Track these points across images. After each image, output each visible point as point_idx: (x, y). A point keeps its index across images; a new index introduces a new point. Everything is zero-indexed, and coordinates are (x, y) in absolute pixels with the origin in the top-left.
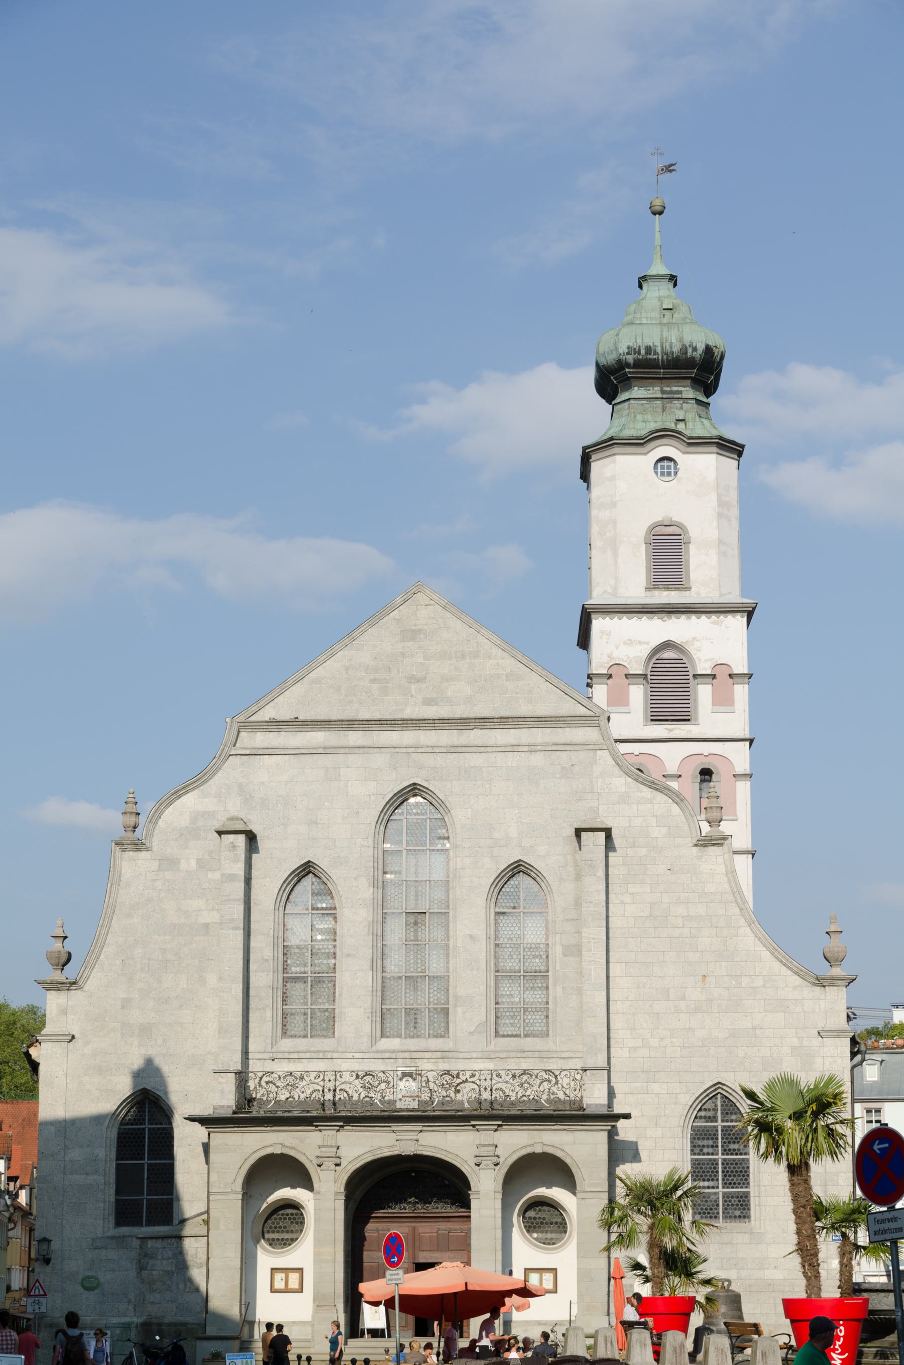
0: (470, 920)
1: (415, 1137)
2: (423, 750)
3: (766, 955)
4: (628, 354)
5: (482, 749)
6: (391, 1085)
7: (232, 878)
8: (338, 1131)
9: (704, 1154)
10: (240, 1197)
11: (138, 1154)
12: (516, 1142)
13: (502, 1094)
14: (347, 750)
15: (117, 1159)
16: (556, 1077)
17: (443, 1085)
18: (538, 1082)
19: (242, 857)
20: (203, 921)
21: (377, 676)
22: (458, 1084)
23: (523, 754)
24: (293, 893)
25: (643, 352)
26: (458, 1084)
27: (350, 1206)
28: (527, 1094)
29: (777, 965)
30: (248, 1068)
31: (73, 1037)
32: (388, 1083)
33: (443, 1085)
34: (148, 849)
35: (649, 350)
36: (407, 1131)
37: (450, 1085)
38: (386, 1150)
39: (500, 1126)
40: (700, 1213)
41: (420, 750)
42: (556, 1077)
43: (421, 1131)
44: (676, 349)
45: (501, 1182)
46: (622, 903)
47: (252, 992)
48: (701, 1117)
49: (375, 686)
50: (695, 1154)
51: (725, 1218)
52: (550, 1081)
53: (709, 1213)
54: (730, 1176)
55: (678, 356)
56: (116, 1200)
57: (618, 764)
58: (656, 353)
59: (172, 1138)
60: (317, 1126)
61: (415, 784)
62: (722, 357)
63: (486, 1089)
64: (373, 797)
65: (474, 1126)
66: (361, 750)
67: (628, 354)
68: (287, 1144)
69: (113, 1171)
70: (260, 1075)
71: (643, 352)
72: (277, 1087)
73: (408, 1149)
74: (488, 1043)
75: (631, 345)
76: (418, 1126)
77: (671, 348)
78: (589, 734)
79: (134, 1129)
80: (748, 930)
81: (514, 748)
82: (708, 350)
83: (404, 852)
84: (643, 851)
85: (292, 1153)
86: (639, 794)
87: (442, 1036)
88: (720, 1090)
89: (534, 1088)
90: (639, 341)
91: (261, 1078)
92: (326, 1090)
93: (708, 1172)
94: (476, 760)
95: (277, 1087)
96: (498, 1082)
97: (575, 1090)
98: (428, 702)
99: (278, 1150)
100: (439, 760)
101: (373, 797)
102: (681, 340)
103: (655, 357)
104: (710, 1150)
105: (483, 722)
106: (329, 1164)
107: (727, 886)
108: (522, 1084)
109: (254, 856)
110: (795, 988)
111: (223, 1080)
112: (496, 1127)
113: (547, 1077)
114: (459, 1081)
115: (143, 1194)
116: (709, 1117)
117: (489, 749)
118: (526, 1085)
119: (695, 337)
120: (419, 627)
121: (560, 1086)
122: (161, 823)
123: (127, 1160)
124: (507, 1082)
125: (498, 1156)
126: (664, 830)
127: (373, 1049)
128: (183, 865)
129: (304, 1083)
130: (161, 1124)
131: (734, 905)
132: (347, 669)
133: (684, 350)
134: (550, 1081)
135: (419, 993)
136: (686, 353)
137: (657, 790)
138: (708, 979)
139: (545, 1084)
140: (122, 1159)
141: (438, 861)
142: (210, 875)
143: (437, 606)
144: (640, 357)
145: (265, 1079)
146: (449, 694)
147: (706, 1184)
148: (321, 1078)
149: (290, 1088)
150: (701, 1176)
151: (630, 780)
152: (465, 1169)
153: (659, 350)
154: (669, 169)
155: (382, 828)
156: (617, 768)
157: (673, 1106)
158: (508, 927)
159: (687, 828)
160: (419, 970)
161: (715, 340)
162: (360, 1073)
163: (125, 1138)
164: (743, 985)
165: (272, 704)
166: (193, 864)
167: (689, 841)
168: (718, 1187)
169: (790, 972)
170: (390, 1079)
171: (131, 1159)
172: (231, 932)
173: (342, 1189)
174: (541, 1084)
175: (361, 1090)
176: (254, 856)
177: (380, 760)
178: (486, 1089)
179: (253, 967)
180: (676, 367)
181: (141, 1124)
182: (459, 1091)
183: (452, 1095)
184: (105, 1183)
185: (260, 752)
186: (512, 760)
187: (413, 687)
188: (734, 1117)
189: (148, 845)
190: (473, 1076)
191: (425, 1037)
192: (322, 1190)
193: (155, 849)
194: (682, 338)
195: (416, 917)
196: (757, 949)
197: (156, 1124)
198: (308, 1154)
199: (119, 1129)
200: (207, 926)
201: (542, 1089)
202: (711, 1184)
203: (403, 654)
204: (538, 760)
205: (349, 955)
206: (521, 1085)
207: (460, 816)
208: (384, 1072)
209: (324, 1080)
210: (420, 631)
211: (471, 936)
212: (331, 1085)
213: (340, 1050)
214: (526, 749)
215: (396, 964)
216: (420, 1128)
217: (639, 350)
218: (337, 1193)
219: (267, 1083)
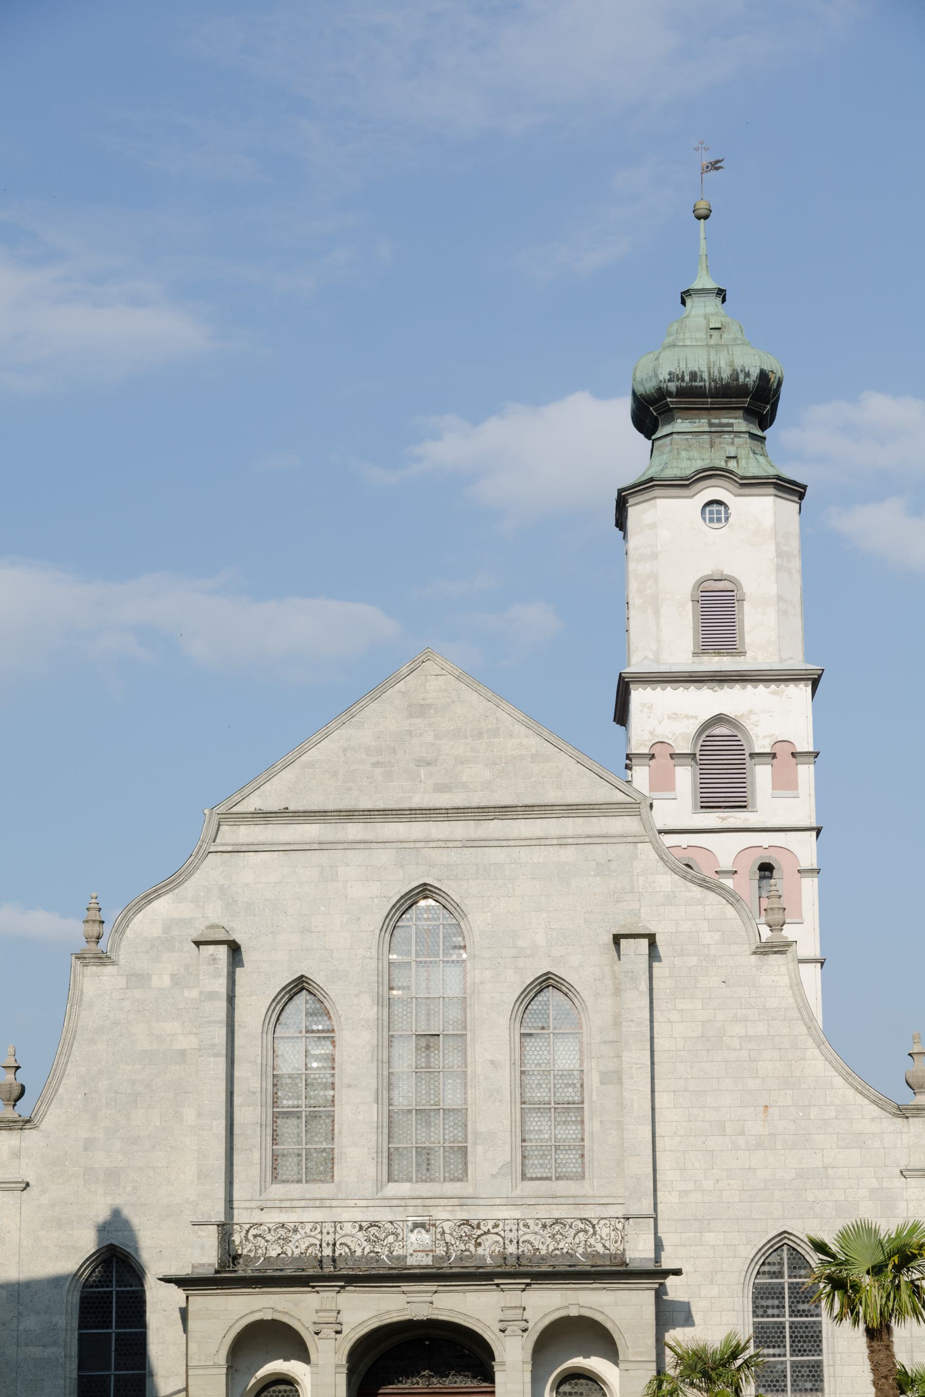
0: (491, 1043)
1: (429, 1299)
2: (434, 844)
3: (839, 1081)
4: (670, 381)
5: (503, 843)
6: (400, 1238)
7: (212, 996)
8: (339, 1292)
9: (768, 1316)
10: (224, 1371)
11: (105, 1322)
12: (547, 1304)
13: (530, 1248)
14: (346, 846)
15: (80, 1328)
16: (594, 1227)
17: (461, 1237)
19: (224, 971)
20: (179, 1047)
21: (380, 758)
22: (479, 1236)
23: (551, 849)
24: (284, 1014)
25: (687, 378)
26: (479, 1236)
27: (353, 1380)
28: (560, 1247)
29: (851, 1092)
30: (232, 1219)
31: (28, 1185)
32: (397, 1235)
33: (461, 1237)
34: (113, 963)
35: (694, 376)
36: (419, 1292)
37: (469, 1236)
38: (394, 1315)
39: (528, 1284)
40: (764, 1386)
41: (431, 844)
42: (594, 1227)
43: (436, 1292)
44: (726, 375)
45: (530, 1351)
46: (669, 1021)
47: (237, 1130)
48: (764, 1273)
49: (378, 770)
51: (794, 1391)
52: (586, 1231)
53: (775, 1386)
54: (799, 1341)
55: (727, 383)
56: (79, 1376)
57: (662, 859)
58: (702, 380)
59: (145, 1302)
60: (313, 1287)
61: (425, 884)
62: (780, 384)
63: (511, 1241)
64: (376, 901)
65: (497, 1285)
66: (362, 845)
67: (670, 381)
68: (279, 1308)
69: (75, 1342)
70: (247, 1227)
71: (687, 378)
72: (267, 1241)
74: (514, 1187)
75: (673, 370)
77: (720, 373)
78: (630, 824)
79: (99, 1292)
80: (817, 1052)
81: (540, 841)
82: (763, 375)
83: (414, 964)
84: (693, 961)
85: (285, 1319)
86: (688, 894)
87: (460, 1180)
88: (786, 1241)
89: (569, 1240)
90: (683, 366)
91: (248, 1231)
92: (324, 1245)
94: (496, 855)
95: (267, 1241)
96: (525, 1234)
97: (616, 1242)
98: (441, 788)
99: (268, 1316)
100: (454, 856)
101: (376, 901)
102: (731, 364)
103: (702, 384)
104: (776, 1311)
105: (504, 811)
106: (328, 1331)
107: (791, 1000)
108: (554, 1235)
109: (238, 970)
110: (873, 1119)
111: (203, 1234)
112: (523, 1286)
113: (582, 1226)
114: (479, 1232)
115: (110, 1369)
116: (774, 1273)
117: (512, 843)
118: (558, 1237)
119: (748, 361)
120: (429, 701)
122: (129, 933)
123: (91, 1328)
124: (536, 1233)
125: (526, 1321)
126: (717, 936)
127: (379, 1195)
128: (155, 982)
129: (298, 1236)
130: (131, 1286)
131: (800, 1022)
132: (345, 750)
133: (735, 376)
134: (586, 1231)
135: (432, 1129)
136: (737, 379)
137: (708, 888)
138: (770, 1110)
139: (581, 1234)
140: (86, 1328)
141: (453, 973)
142: (186, 993)
143: (449, 676)
144: (684, 384)
145: (253, 1232)
146: (464, 779)
147: (771, 1351)
148: (319, 1230)
149: (281, 1242)
150: (766, 1342)
151: (676, 876)
152: (488, 1336)
153: (706, 376)
154: (715, 166)
155: (388, 936)
156: (661, 864)
157: (731, 1260)
158: (536, 1052)
159: (744, 933)
160: (432, 1102)
161: (771, 364)
162: (363, 1224)
163: (88, 1303)
164: (812, 1117)
165: (257, 792)
166: (167, 980)
167: (747, 949)
169: (866, 1102)
170: (399, 1231)
171: (97, 1328)
172: (212, 1059)
173: (344, 1361)
174: (576, 1235)
175: (365, 1244)
176: (238, 970)
177: (384, 856)
178: (511, 1241)
179: (237, 1100)
180: (725, 396)
181: (108, 1286)
182: (480, 1244)
184: (65, 1356)
185: (244, 849)
186: (538, 855)
187: (422, 771)
188: (803, 1272)
189: (114, 958)
190: (496, 1226)
191: (439, 1181)
192: (321, 1362)
193: (122, 962)
194: (733, 362)
195: (428, 1041)
196: (828, 1074)
197: (125, 1286)
198: (303, 1320)
199: (82, 1292)
200: (183, 1052)
201: (577, 1240)
202: (777, 1351)
203: (410, 733)
204: (569, 854)
205: (350, 1086)
206: (553, 1237)
207: (478, 921)
209: (321, 1232)
210: (429, 706)
211: (492, 1062)
212: (330, 1239)
213: (340, 1196)
214: (555, 842)
215: (406, 1094)
216: (435, 1288)
217: (683, 376)
218: (337, 1366)
219: (255, 1236)
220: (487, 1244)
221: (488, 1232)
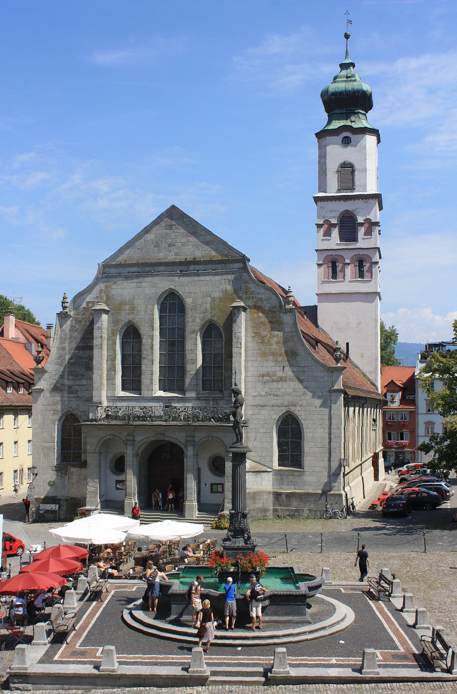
190: (185, 409)
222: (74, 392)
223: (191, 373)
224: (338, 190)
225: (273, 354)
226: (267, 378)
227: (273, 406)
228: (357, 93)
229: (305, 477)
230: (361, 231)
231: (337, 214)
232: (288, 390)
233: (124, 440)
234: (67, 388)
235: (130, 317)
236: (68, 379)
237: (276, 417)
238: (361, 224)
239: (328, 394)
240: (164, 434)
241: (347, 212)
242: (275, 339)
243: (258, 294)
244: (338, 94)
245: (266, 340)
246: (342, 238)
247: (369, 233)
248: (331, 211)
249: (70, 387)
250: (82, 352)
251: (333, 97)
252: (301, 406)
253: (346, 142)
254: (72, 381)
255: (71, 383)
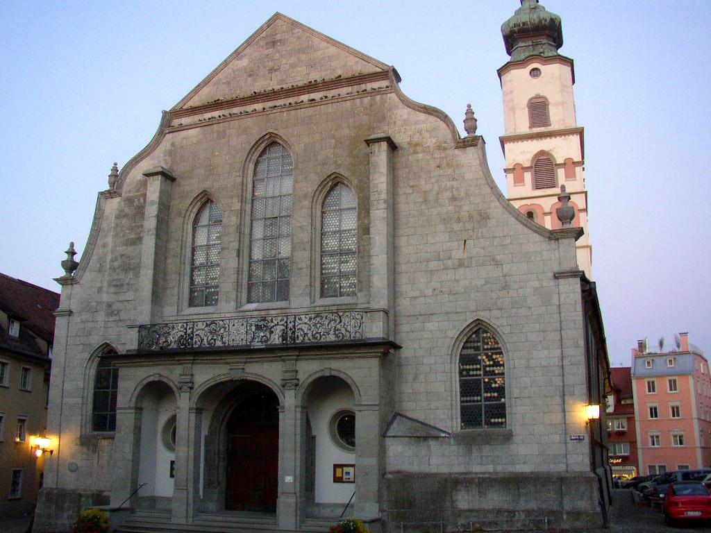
16: (340, 317)
18: (326, 322)
39: (298, 356)
42: (340, 317)
43: (246, 363)
50: (463, 376)
73: (237, 375)
76: (242, 358)
80: (497, 204)
93: (473, 389)
96: (300, 324)
97: (355, 327)
114: (273, 324)
121: (342, 324)
124: (306, 323)
125: (298, 380)
134: (335, 321)
152: (276, 390)
164: (495, 244)
168: (481, 401)
169: (531, 232)
170: (227, 326)
182: (272, 332)
183: (268, 335)
206: (315, 325)
208: (223, 321)
220: (277, 332)
221: (277, 324)
222: (116, 312)
223: (300, 266)
224: (530, 128)
225: (445, 221)
226: (436, 263)
227: (447, 313)
228: (543, 21)
229: (513, 447)
230: (561, 173)
231: (530, 156)
232: (475, 282)
233: (176, 383)
234: (104, 306)
235: (207, 185)
236: (108, 293)
237: (454, 333)
238: (564, 165)
239: (552, 283)
240: (243, 369)
241: (542, 153)
242: (448, 195)
243: (416, 124)
244: (521, 25)
245: (431, 198)
246: (537, 186)
247: (571, 175)
248: (523, 153)
249: (109, 305)
250: (130, 248)
251: (516, 29)
252: (501, 309)
253: (535, 72)
254: (113, 296)
255: (112, 298)
